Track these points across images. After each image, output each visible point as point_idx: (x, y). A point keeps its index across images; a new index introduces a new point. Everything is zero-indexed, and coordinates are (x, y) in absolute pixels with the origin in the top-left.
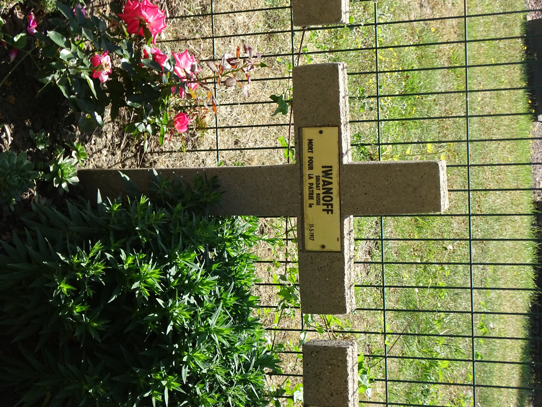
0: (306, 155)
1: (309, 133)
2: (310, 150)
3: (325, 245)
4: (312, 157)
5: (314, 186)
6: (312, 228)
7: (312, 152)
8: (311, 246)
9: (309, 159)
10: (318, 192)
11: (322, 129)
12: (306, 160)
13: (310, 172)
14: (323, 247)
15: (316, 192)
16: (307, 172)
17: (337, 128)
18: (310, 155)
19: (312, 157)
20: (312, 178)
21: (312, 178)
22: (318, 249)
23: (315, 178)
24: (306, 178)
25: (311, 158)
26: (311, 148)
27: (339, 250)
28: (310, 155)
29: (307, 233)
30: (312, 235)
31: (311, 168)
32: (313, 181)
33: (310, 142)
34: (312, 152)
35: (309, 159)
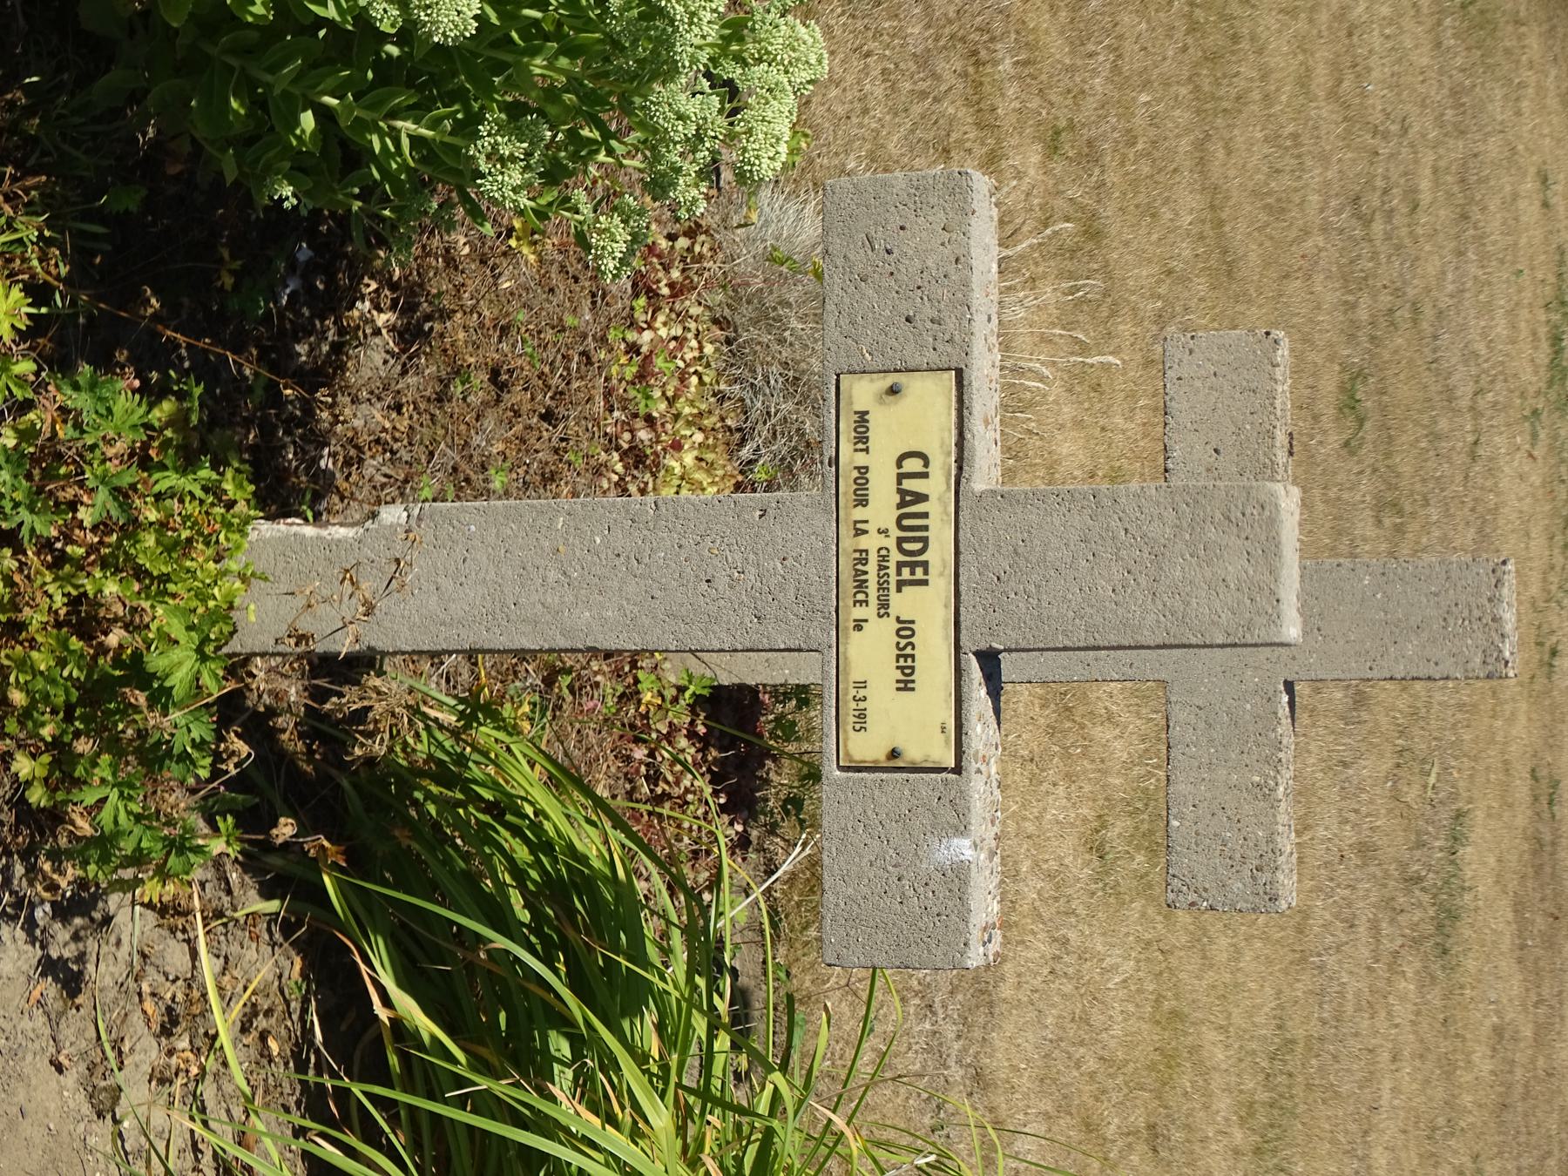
2: (860, 446)
3: (900, 744)
4: (867, 468)
6: (862, 693)
7: (867, 450)
9: (855, 474)
13: (859, 514)
14: (894, 754)
18: (861, 460)
19: (867, 468)
20: (866, 532)
21: (866, 532)
25: (863, 470)
26: (862, 439)
30: (862, 715)
31: (862, 502)
33: (862, 417)
34: (867, 450)
35: (855, 474)
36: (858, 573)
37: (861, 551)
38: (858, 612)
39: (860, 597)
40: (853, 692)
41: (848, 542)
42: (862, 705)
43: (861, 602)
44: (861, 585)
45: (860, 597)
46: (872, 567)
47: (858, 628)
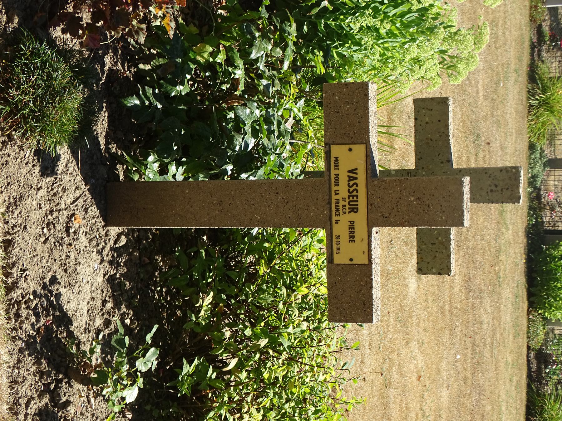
0: (333, 172)
1: (336, 150)
7: (338, 169)
8: (338, 259)
11: (348, 147)
12: (333, 176)
13: (336, 188)
14: (351, 260)
16: (334, 188)
17: (363, 146)
18: (337, 172)
24: (333, 193)
25: (337, 175)
26: (336, 165)
27: (367, 262)
28: (337, 172)
29: (335, 246)
30: (338, 249)
31: (337, 184)
33: (336, 159)
34: (338, 169)
36: (336, 206)
39: (337, 213)
40: (336, 240)
41: (334, 197)
42: (339, 246)
43: (337, 215)
44: (337, 210)
46: (341, 205)
47: (337, 222)
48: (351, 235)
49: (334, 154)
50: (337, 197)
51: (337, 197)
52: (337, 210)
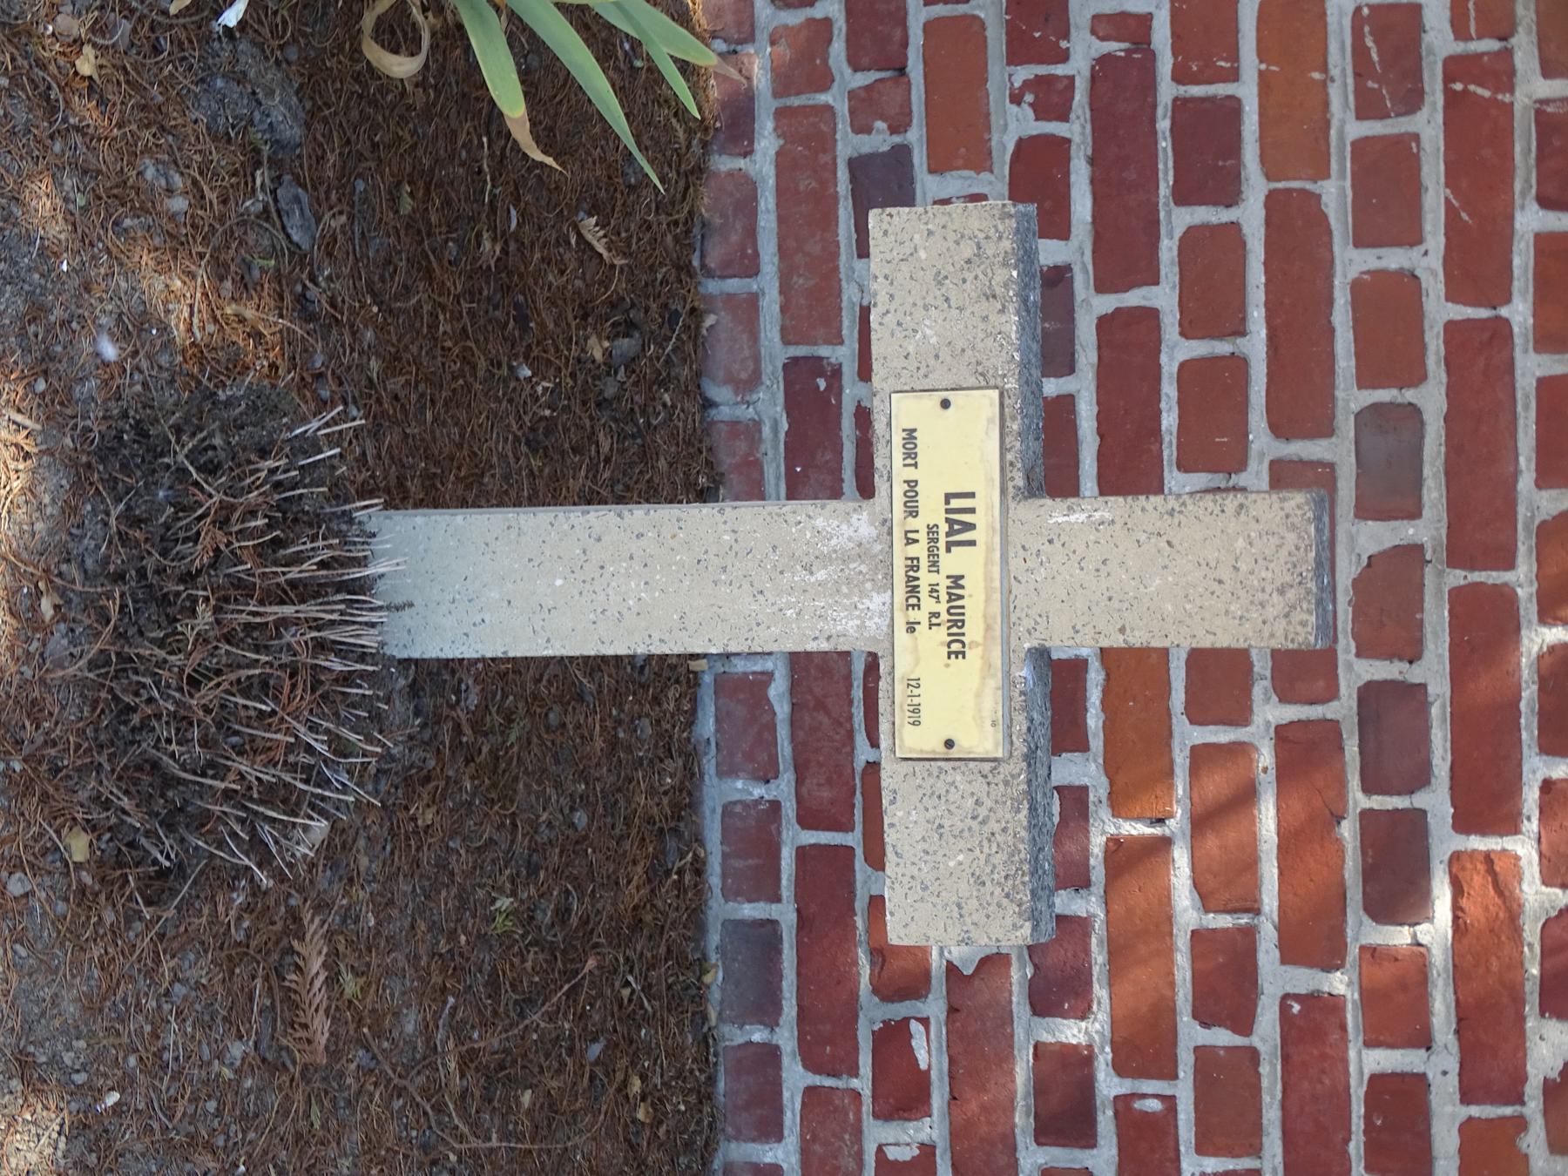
0: (901, 473)
2: (909, 461)
5: (924, 563)
7: (916, 465)
10: (934, 578)
13: (912, 523)
14: (949, 744)
15: (925, 578)
18: (910, 473)
22: (934, 746)
23: (922, 536)
25: (912, 484)
26: (911, 455)
28: (910, 473)
30: (916, 710)
31: (913, 512)
32: (920, 550)
33: (910, 434)
36: (910, 579)
37: (912, 559)
38: (914, 615)
39: (913, 601)
42: (916, 700)
44: (913, 590)
45: (913, 601)
47: (911, 628)
48: (955, 630)
49: (901, 422)
50: (913, 550)
51: (913, 550)
52: (913, 590)
